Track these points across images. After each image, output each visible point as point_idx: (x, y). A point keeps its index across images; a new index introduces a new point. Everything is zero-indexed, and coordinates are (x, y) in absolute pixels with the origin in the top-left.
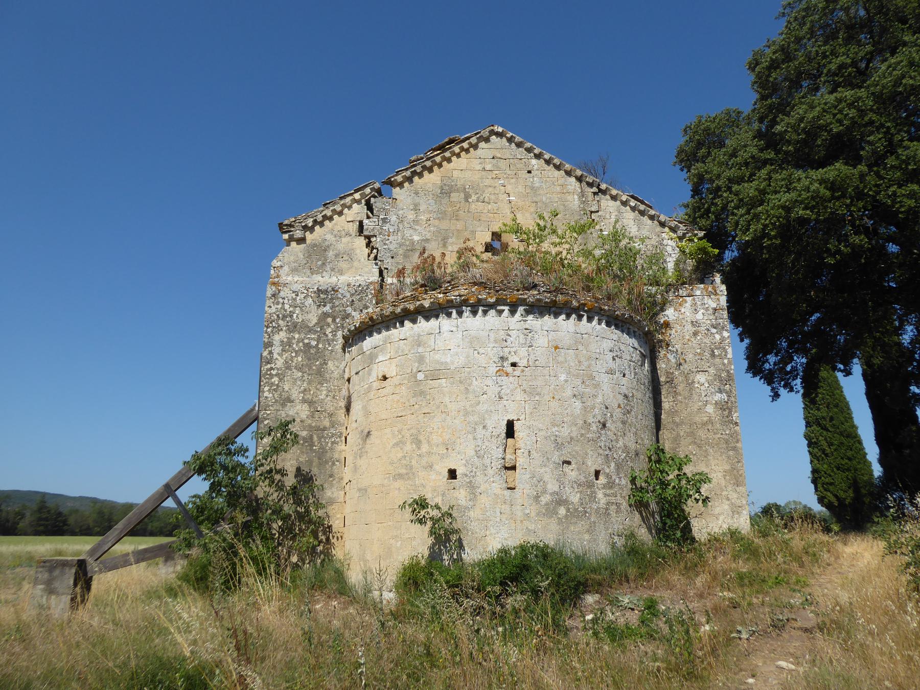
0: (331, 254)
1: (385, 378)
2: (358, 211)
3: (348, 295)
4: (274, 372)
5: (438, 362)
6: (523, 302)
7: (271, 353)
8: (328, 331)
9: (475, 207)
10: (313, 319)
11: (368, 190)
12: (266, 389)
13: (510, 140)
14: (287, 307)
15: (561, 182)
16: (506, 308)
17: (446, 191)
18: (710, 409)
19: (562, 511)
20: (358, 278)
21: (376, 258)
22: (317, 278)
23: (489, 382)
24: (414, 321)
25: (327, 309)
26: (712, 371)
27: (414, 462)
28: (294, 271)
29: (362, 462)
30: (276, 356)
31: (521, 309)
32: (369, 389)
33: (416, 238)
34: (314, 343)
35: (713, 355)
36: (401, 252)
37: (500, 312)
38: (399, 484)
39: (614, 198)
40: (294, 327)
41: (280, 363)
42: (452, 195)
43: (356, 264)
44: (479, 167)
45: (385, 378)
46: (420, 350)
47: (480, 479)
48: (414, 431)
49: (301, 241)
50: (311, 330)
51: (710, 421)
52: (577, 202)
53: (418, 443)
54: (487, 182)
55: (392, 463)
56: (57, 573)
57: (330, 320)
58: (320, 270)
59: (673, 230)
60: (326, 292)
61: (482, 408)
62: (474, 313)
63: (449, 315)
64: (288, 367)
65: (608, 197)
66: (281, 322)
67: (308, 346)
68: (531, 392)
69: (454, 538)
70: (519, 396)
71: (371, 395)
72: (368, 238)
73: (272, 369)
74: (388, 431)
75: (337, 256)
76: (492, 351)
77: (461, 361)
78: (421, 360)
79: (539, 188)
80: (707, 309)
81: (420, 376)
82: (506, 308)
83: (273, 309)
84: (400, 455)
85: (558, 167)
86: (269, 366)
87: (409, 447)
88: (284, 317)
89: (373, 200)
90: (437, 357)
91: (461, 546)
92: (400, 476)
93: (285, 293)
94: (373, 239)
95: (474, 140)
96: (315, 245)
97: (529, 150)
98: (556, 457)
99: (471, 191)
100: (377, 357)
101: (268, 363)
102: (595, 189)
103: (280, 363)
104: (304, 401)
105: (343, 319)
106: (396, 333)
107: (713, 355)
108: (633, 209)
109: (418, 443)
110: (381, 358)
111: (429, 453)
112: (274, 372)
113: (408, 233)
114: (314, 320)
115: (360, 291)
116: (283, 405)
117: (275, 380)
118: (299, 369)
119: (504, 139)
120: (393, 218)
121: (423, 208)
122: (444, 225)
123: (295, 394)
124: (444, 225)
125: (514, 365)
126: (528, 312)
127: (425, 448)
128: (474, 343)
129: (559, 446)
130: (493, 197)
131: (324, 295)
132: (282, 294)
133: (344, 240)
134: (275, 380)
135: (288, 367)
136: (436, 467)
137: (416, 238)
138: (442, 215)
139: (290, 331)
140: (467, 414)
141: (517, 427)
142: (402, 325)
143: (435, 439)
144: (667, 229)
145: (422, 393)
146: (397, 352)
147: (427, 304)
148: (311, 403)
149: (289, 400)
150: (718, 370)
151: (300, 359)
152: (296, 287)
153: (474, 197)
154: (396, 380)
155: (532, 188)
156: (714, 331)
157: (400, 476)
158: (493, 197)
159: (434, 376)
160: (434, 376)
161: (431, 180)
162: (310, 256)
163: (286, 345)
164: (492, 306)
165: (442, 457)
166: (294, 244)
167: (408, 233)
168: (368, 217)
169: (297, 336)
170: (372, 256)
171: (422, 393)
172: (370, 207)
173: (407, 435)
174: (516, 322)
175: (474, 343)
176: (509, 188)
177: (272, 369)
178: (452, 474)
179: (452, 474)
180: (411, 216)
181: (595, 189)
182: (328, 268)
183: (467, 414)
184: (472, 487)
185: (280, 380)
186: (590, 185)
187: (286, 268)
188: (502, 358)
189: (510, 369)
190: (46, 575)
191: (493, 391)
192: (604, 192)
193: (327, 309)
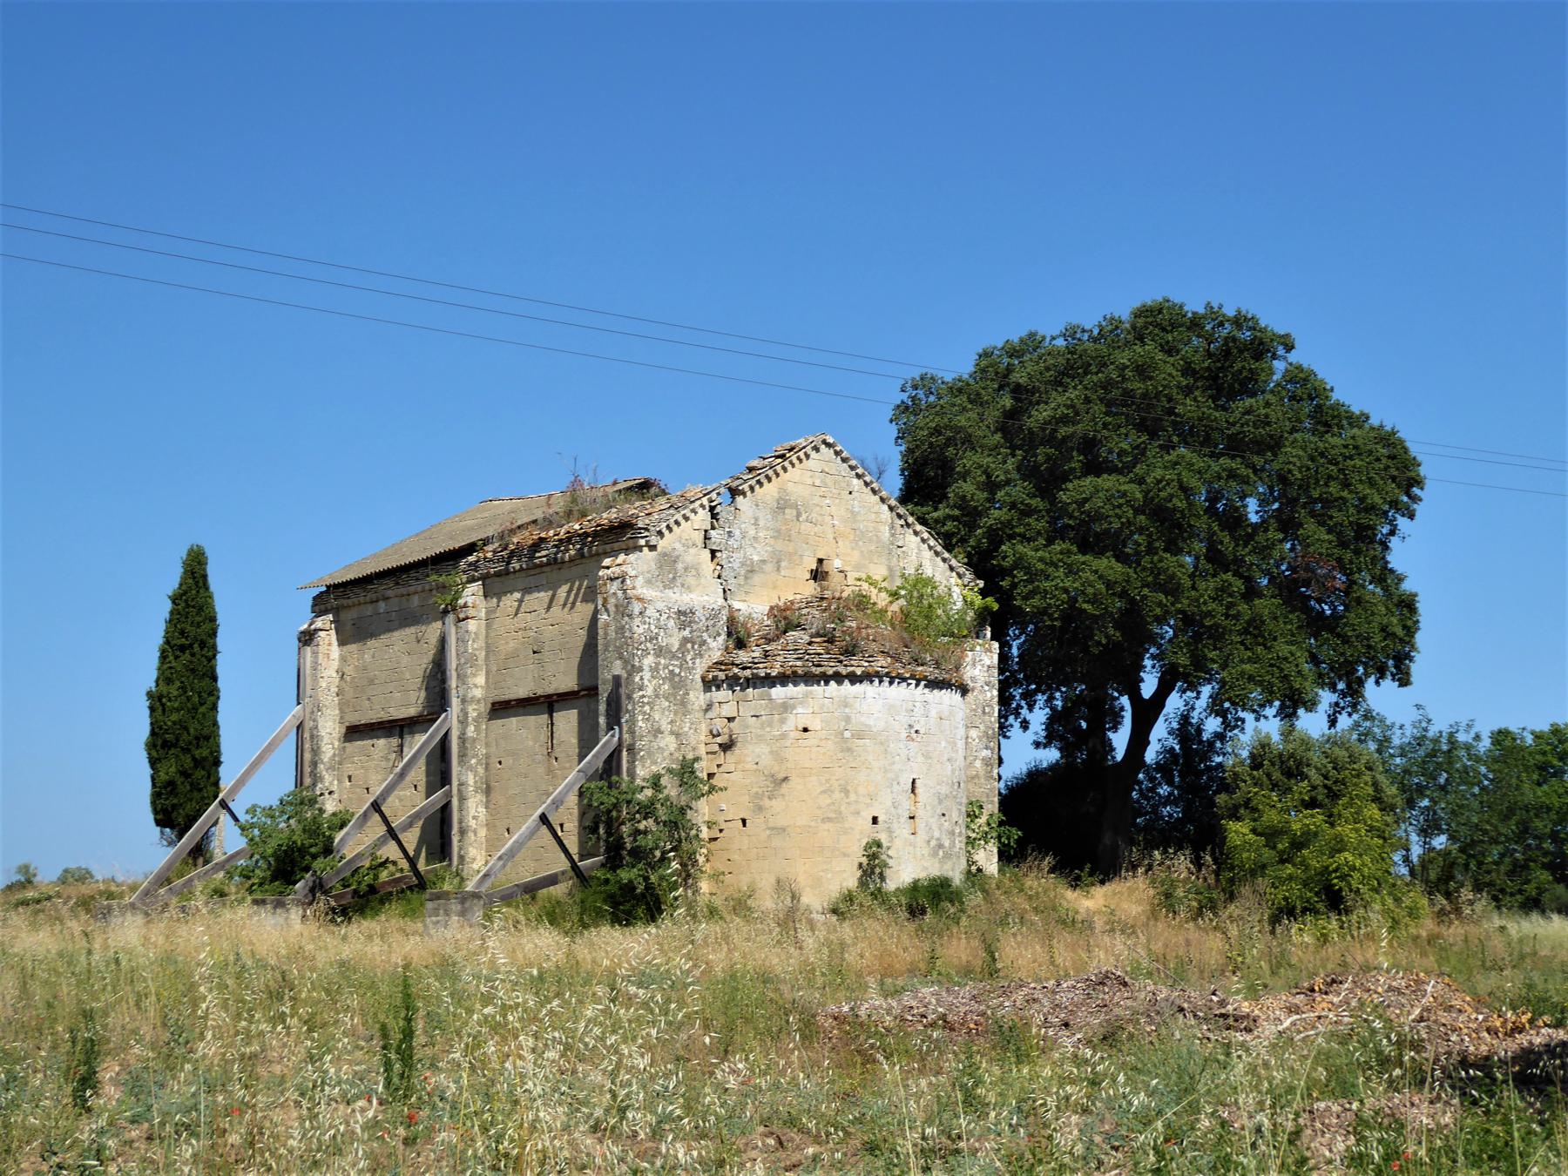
0: (680, 566)
1: (805, 730)
2: (702, 518)
3: (703, 619)
4: (646, 700)
5: (863, 724)
6: (925, 678)
7: (642, 679)
8: (689, 657)
9: (806, 527)
10: (675, 644)
11: (714, 495)
12: (640, 718)
13: (837, 453)
14: (653, 627)
15: (876, 508)
16: (914, 682)
17: (782, 506)
18: (978, 764)
19: (941, 853)
20: (706, 598)
21: (719, 577)
22: (669, 593)
23: (901, 745)
24: (840, 683)
25: (686, 633)
26: (982, 727)
27: (843, 808)
28: (649, 582)
29: (776, 804)
30: (646, 682)
31: (923, 683)
32: (784, 736)
33: (756, 558)
34: (677, 671)
35: (984, 712)
36: (743, 572)
37: (909, 684)
38: (828, 826)
39: (916, 533)
40: (660, 652)
41: (649, 691)
42: (787, 511)
43: (703, 580)
44: (809, 481)
45: (805, 730)
46: (847, 710)
47: (895, 826)
48: (842, 782)
49: (653, 548)
50: (674, 657)
51: (977, 776)
52: (887, 534)
53: (846, 792)
54: (817, 500)
55: (819, 808)
56: (467, 905)
57: (689, 646)
58: (670, 584)
59: (960, 576)
60: (684, 613)
61: (897, 767)
62: (891, 683)
63: (872, 682)
64: (657, 696)
65: (911, 531)
66: (648, 644)
67: (672, 672)
68: (927, 756)
69: (878, 870)
70: (920, 759)
71: (788, 743)
72: (713, 553)
73: (643, 696)
74: (814, 778)
75: (686, 569)
76: (904, 720)
77: (881, 725)
78: (848, 719)
79: (859, 512)
80: (983, 666)
81: (847, 734)
82: (914, 682)
83: (641, 630)
84: (829, 801)
85: (874, 492)
86: (641, 693)
87: (837, 795)
88: (651, 639)
89: (718, 509)
90: (863, 719)
91: (882, 877)
92: (829, 819)
93: (651, 612)
94: (718, 554)
95: (808, 449)
96: (665, 555)
97: (852, 468)
98: (939, 812)
99: (802, 509)
100: (794, 707)
101: (640, 690)
102: (902, 522)
103: (649, 691)
104: (672, 733)
105: (700, 646)
106: (818, 690)
107: (984, 712)
108: (930, 548)
109: (846, 792)
110: (800, 710)
111: (856, 802)
112: (646, 700)
113: (749, 551)
114: (676, 646)
115: (714, 615)
116: (656, 737)
117: (647, 708)
118: (667, 699)
119: (832, 451)
120: (737, 533)
121: (762, 523)
122: (780, 545)
123: (665, 726)
124: (780, 545)
125: (917, 732)
126: (926, 686)
127: (853, 797)
128: (891, 709)
129: (940, 802)
130: (819, 518)
131: (684, 617)
132: (648, 613)
133: (693, 551)
134: (647, 708)
135: (657, 696)
136: (862, 814)
137: (756, 558)
138: (778, 534)
139: (657, 655)
140: (886, 771)
141: (918, 783)
142: (827, 683)
143: (861, 790)
144: (954, 574)
145: (849, 750)
146: (821, 708)
147: (859, 671)
148: (677, 735)
149: (659, 731)
150: (987, 727)
151: (666, 687)
152: (660, 605)
153: (804, 516)
154: (823, 734)
155: (852, 512)
156: (986, 688)
157: (829, 819)
158: (819, 518)
159: (859, 735)
160: (859, 735)
161: (769, 491)
162: (661, 567)
163: (655, 669)
164: (904, 679)
165: (868, 806)
166: (645, 549)
167: (749, 551)
168: (713, 528)
169: (663, 661)
170: (717, 573)
171: (849, 750)
172: (714, 516)
173: (836, 784)
174: (920, 693)
175: (891, 709)
176: (833, 510)
177: (643, 696)
178: (875, 820)
179: (875, 820)
180: (752, 532)
181: (902, 522)
182: (679, 581)
183: (886, 771)
184: (890, 831)
185: (652, 709)
186: (900, 516)
187: (640, 578)
188: (911, 726)
189: (914, 735)
190: (459, 907)
191: (904, 753)
192: (908, 525)
193: (686, 633)
